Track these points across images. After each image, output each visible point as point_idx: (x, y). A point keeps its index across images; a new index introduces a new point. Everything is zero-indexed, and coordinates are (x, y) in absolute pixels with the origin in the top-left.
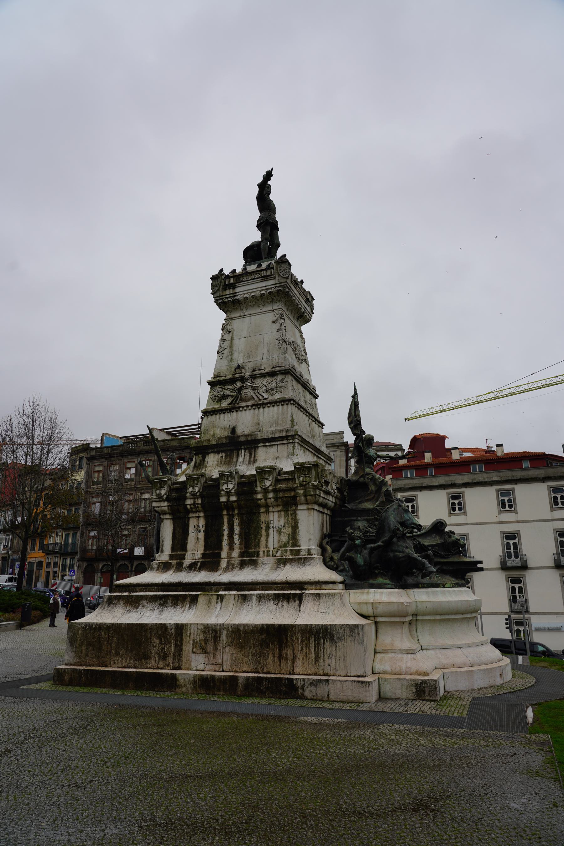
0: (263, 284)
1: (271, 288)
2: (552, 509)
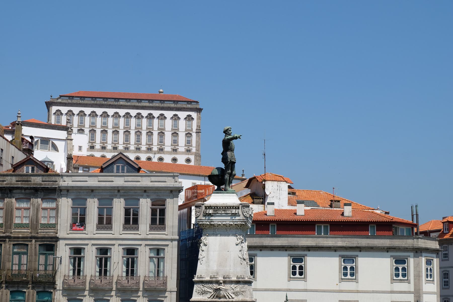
1: (237, 222)
2: (393, 281)
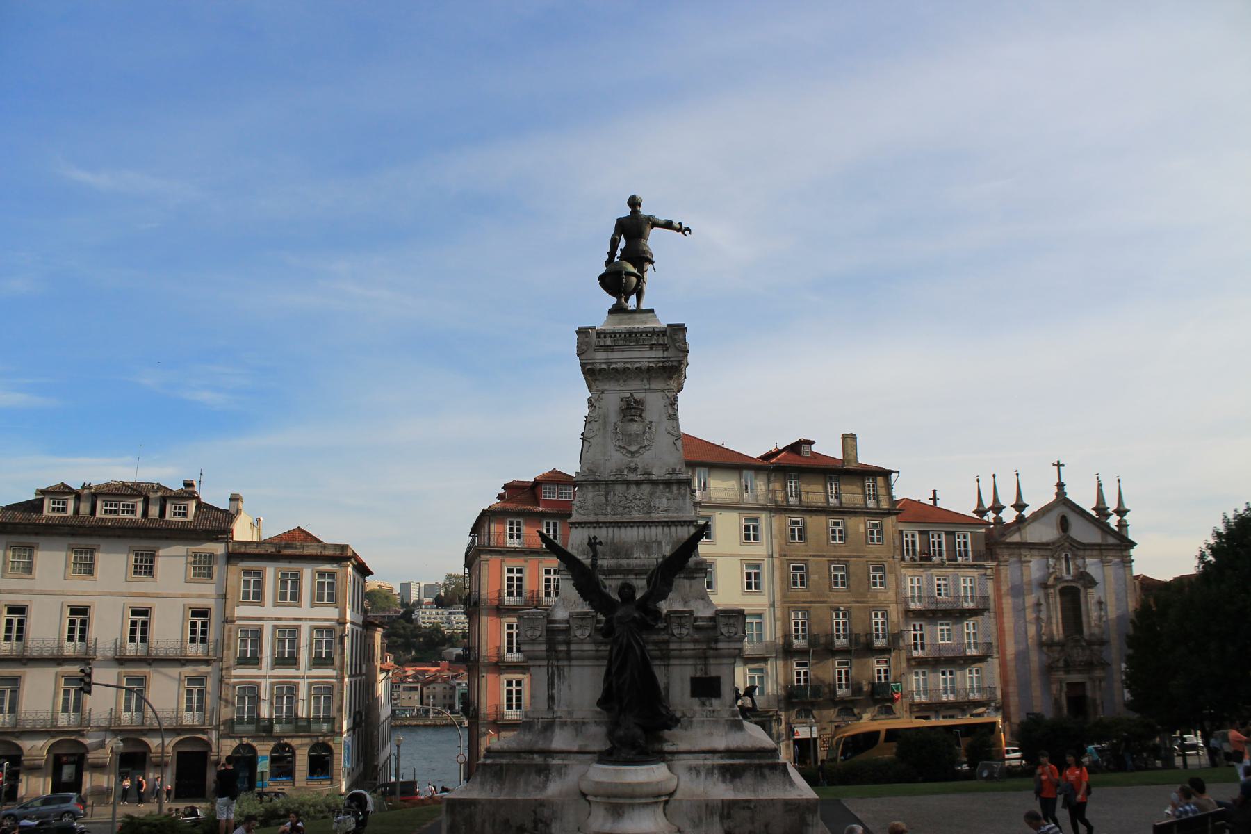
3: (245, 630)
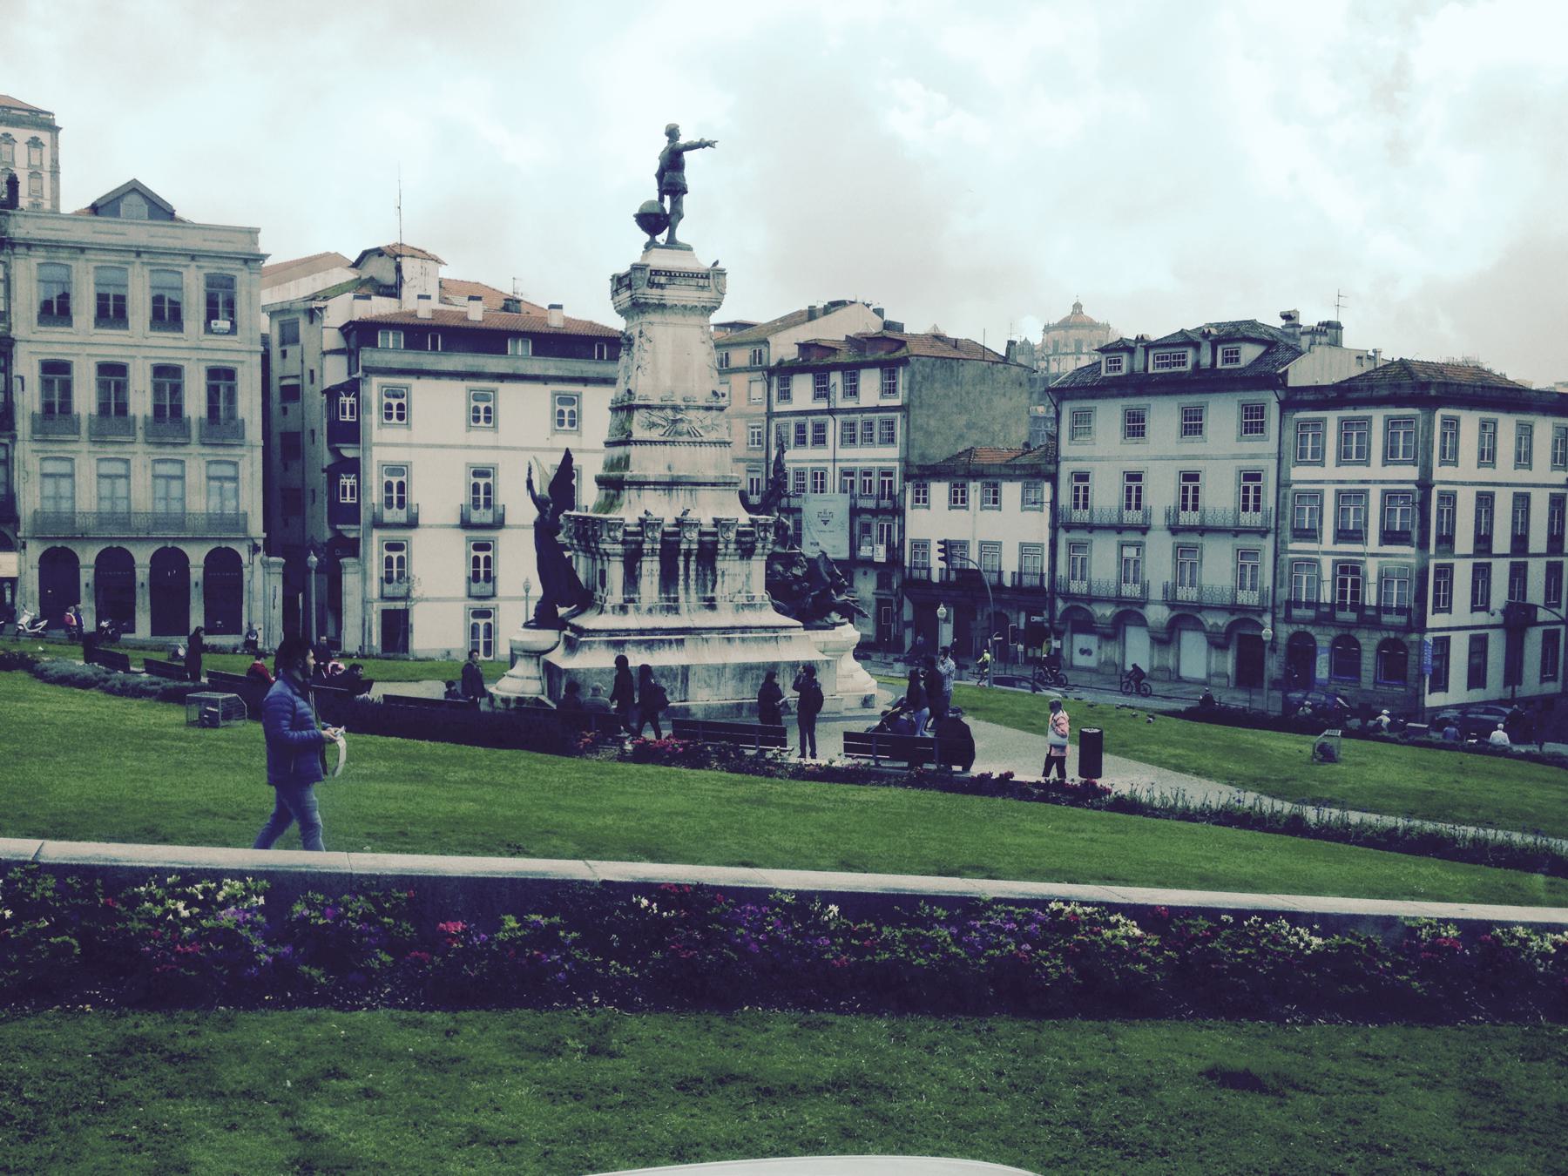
0: (698, 294)
3: (1300, 496)
